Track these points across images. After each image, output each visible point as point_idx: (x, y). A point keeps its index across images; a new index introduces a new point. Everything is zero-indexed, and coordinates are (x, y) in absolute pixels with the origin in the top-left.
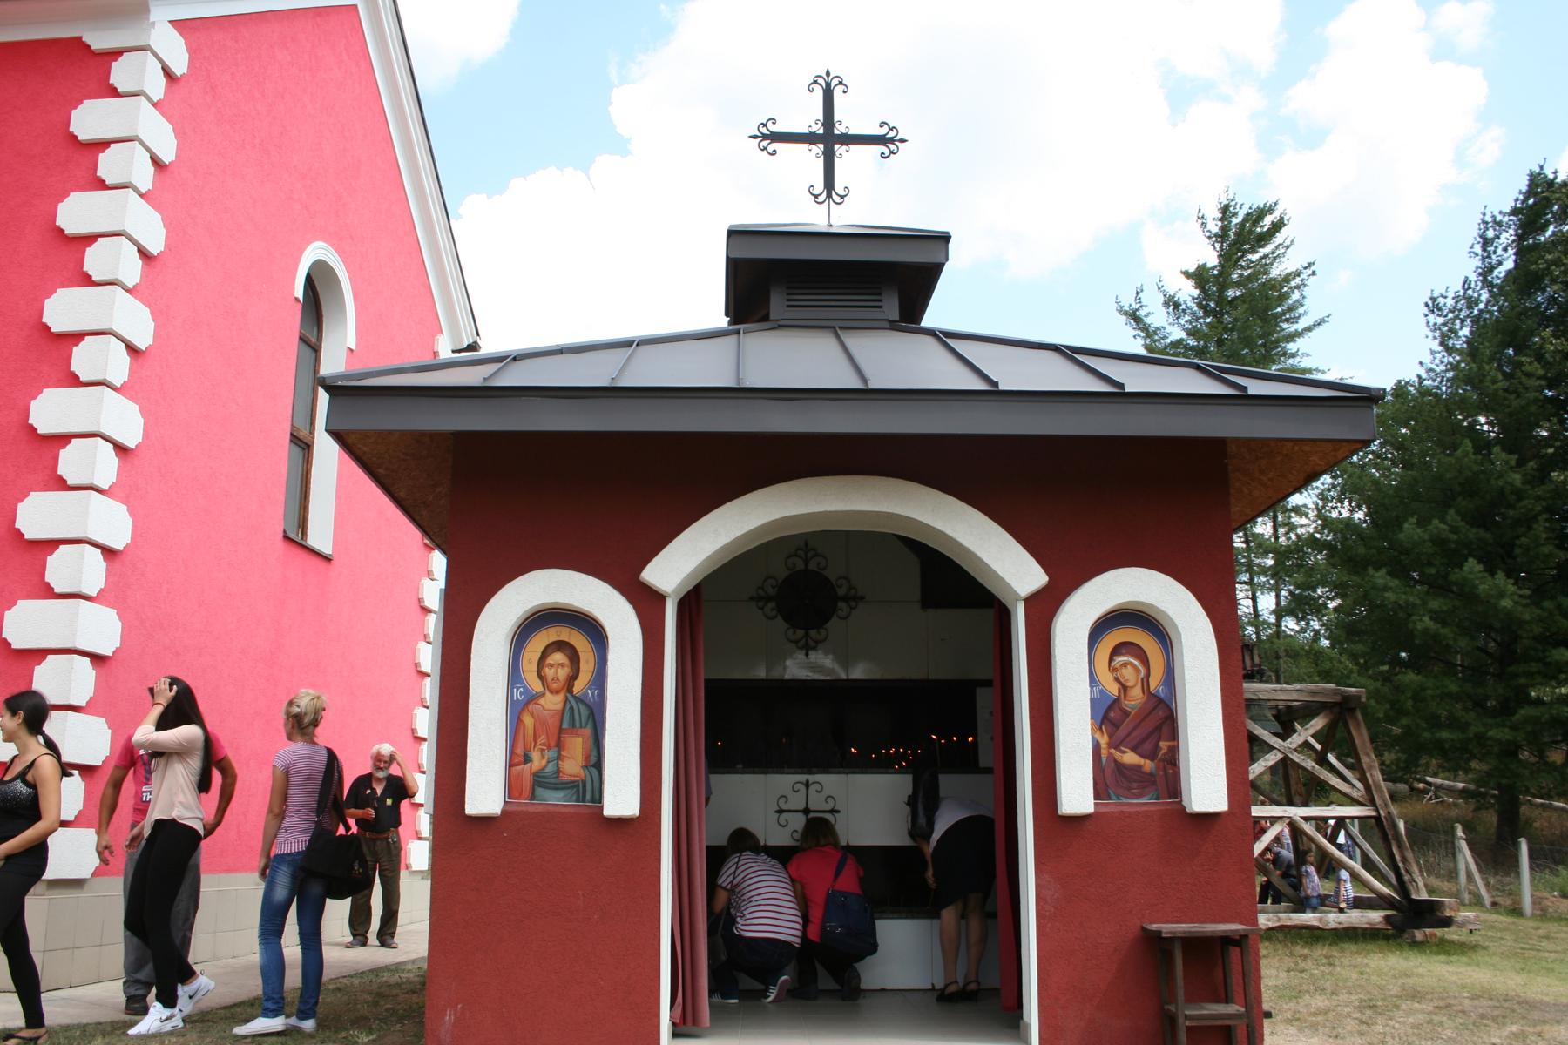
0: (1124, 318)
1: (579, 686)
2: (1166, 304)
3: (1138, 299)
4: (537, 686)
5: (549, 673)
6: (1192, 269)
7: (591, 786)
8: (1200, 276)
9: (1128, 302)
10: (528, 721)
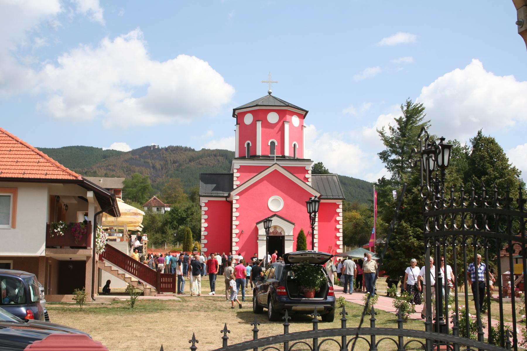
0: (379, 133)
2: (390, 128)
3: (383, 129)
6: (398, 118)
8: (399, 121)
9: (380, 129)
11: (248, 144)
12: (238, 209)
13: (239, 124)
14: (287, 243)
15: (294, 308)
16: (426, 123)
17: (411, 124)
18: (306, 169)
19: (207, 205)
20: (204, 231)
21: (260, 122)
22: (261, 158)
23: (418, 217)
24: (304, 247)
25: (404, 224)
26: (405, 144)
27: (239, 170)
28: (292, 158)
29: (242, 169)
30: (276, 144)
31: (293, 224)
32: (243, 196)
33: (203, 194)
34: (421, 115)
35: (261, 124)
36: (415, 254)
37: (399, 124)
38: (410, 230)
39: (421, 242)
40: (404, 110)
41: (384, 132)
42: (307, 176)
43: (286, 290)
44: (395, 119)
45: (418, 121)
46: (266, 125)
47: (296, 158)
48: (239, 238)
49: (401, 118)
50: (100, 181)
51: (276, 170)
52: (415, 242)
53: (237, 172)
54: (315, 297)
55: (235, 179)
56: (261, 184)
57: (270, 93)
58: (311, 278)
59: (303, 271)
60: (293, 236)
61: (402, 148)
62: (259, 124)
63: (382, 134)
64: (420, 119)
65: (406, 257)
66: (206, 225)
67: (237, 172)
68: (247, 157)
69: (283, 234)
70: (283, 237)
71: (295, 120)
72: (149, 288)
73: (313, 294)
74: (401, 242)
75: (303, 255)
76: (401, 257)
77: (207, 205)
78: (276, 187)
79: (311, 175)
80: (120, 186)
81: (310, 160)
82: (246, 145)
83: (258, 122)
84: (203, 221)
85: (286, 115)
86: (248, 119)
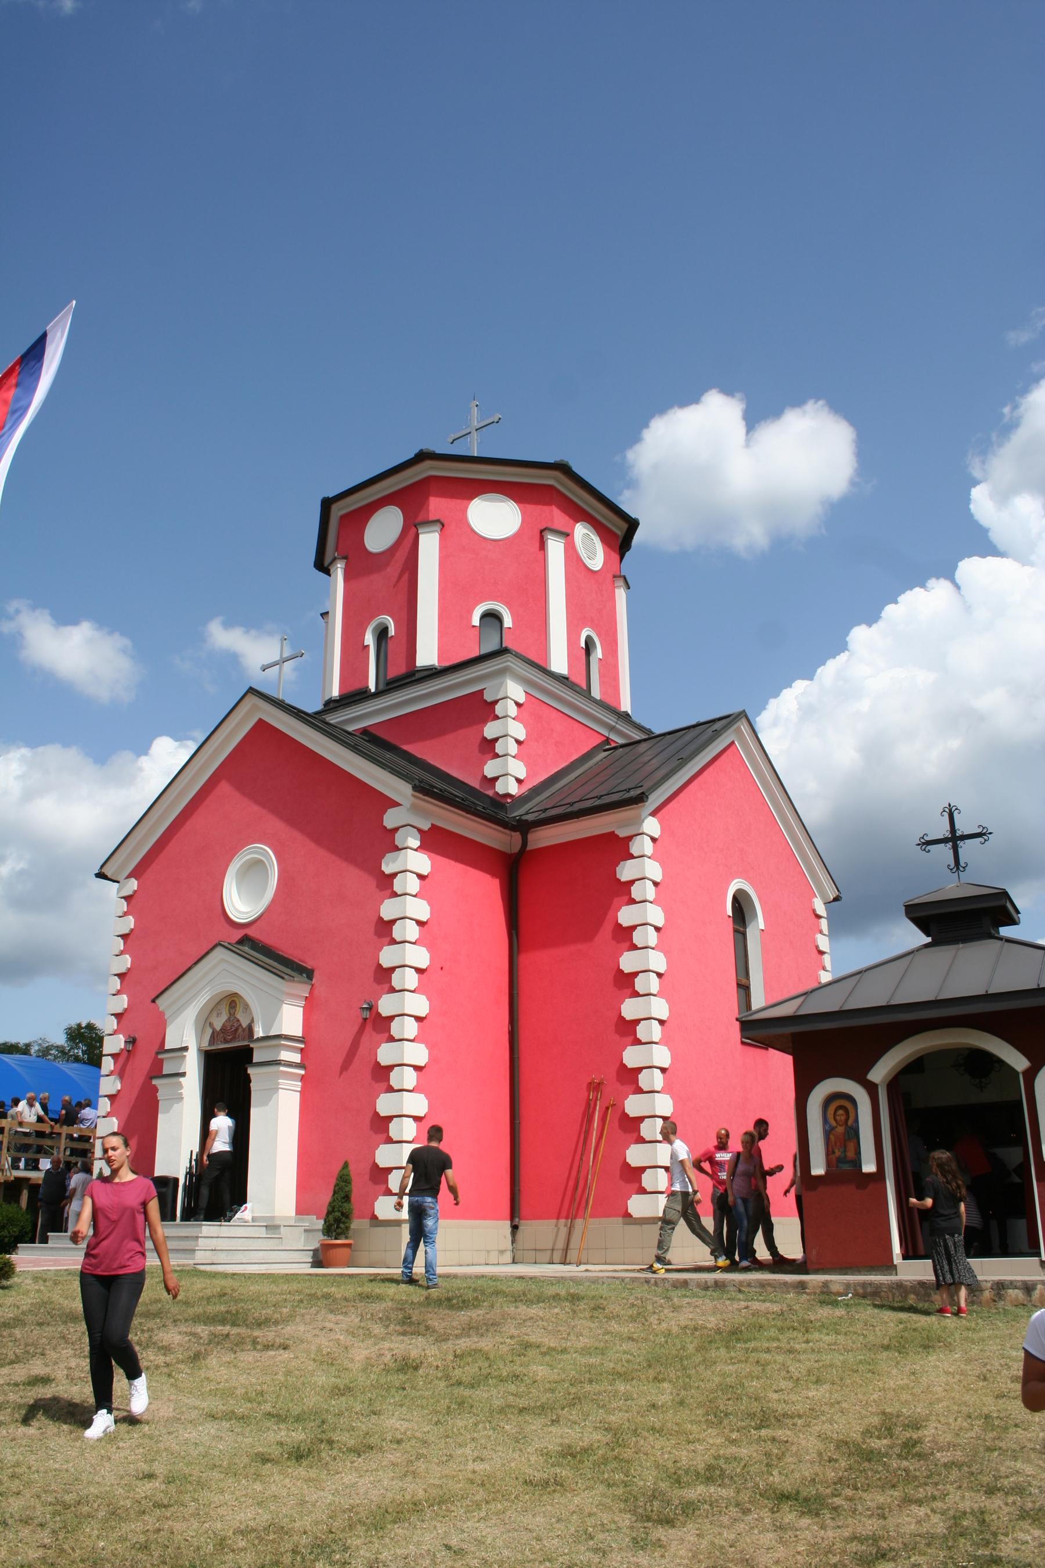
1: (850, 1123)
4: (834, 1124)
5: (838, 1118)
7: (857, 1163)
10: (832, 1137)
30: (392, 632)
32: (149, 873)
51: (261, 722)
85: (427, 498)
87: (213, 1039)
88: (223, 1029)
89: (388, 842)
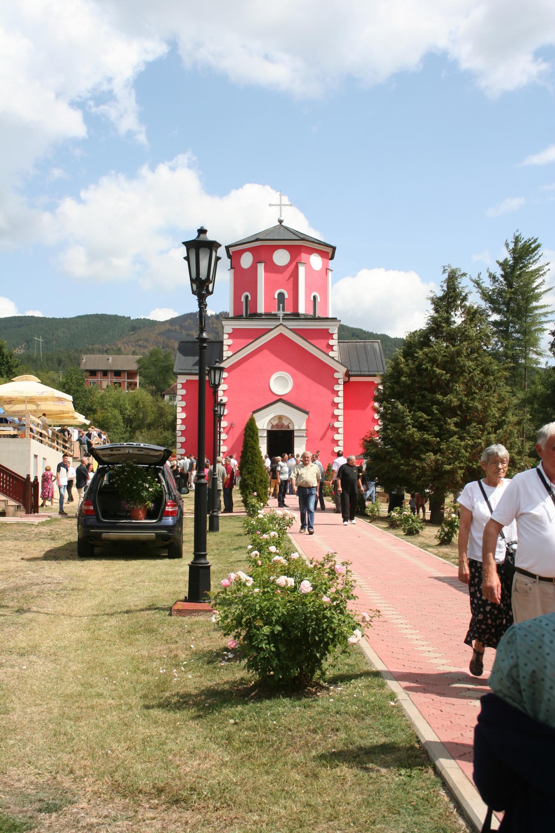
0: (473, 283)
3: (479, 277)
6: (501, 261)
8: (503, 265)
9: (475, 277)
11: (247, 297)
12: (226, 392)
13: (234, 268)
14: (296, 441)
15: (104, 535)
16: (543, 266)
17: (521, 268)
18: (330, 332)
19: (184, 386)
20: (181, 424)
21: (263, 265)
22: (263, 317)
23: (423, 396)
24: (254, 443)
25: (400, 406)
26: (510, 299)
27: (231, 336)
28: (311, 317)
29: (235, 334)
30: (286, 296)
31: (307, 413)
33: (179, 371)
34: (535, 255)
35: (264, 267)
36: (416, 452)
37: (504, 269)
38: (408, 416)
39: (424, 434)
40: (511, 249)
41: (481, 282)
42: (331, 342)
43: (95, 507)
44: (498, 262)
45: (531, 264)
46: (271, 268)
47: (317, 316)
48: (227, 433)
49: (506, 260)
50: (108, 360)
51: (281, 334)
52: (416, 433)
53: (228, 339)
54: (145, 519)
55: (225, 348)
56: (259, 354)
57: (281, 222)
58: (134, 488)
59: (122, 476)
60: (306, 430)
61: (507, 304)
62: (261, 268)
63: (478, 284)
64: (534, 261)
65: (402, 458)
66: (184, 415)
67: (228, 339)
68: (244, 316)
69: (291, 428)
70: (292, 432)
71: (316, 261)
72: (12, 506)
73: (141, 514)
74: (394, 433)
75: (114, 449)
76: (395, 458)
77: (184, 386)
78: (281, 359)
79: (337, 341)
80: (134, 367)
81: (336, 319)
82: (243, 299)
83: (259, 265)
84: (179, 410)
86: (246, 261)
87: (273, 426)
88: (277, 425)
89: (336, 381)
